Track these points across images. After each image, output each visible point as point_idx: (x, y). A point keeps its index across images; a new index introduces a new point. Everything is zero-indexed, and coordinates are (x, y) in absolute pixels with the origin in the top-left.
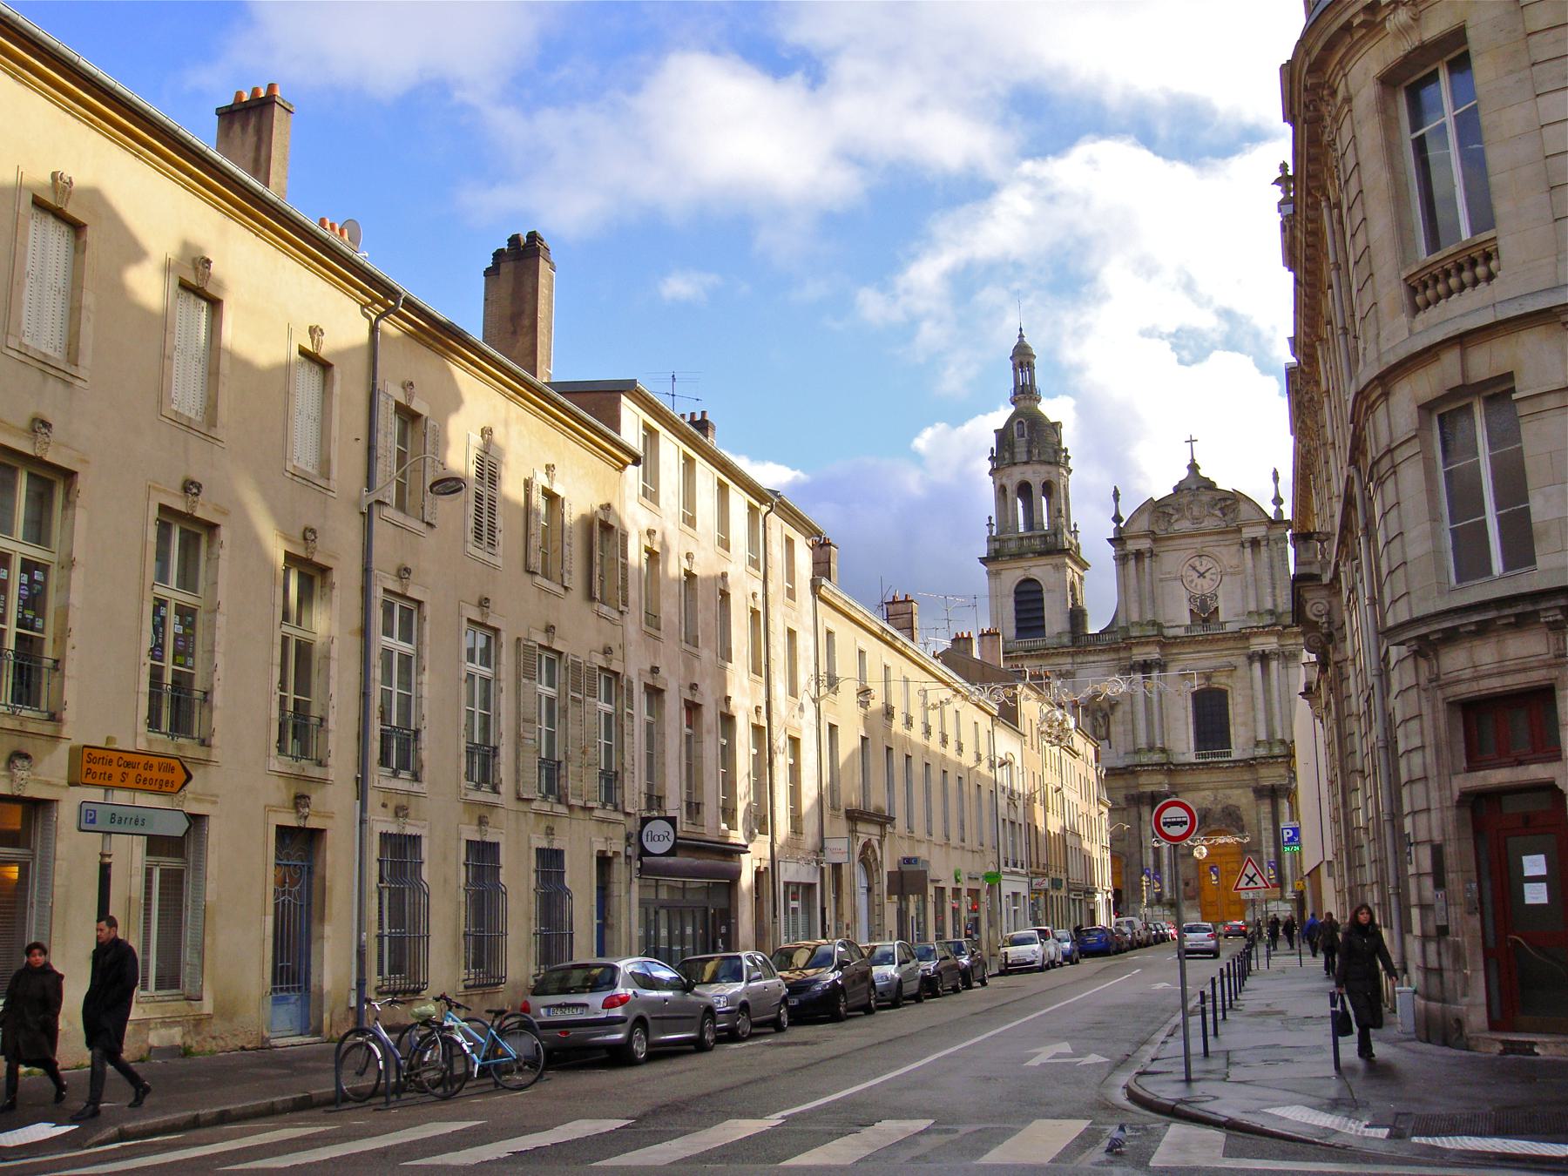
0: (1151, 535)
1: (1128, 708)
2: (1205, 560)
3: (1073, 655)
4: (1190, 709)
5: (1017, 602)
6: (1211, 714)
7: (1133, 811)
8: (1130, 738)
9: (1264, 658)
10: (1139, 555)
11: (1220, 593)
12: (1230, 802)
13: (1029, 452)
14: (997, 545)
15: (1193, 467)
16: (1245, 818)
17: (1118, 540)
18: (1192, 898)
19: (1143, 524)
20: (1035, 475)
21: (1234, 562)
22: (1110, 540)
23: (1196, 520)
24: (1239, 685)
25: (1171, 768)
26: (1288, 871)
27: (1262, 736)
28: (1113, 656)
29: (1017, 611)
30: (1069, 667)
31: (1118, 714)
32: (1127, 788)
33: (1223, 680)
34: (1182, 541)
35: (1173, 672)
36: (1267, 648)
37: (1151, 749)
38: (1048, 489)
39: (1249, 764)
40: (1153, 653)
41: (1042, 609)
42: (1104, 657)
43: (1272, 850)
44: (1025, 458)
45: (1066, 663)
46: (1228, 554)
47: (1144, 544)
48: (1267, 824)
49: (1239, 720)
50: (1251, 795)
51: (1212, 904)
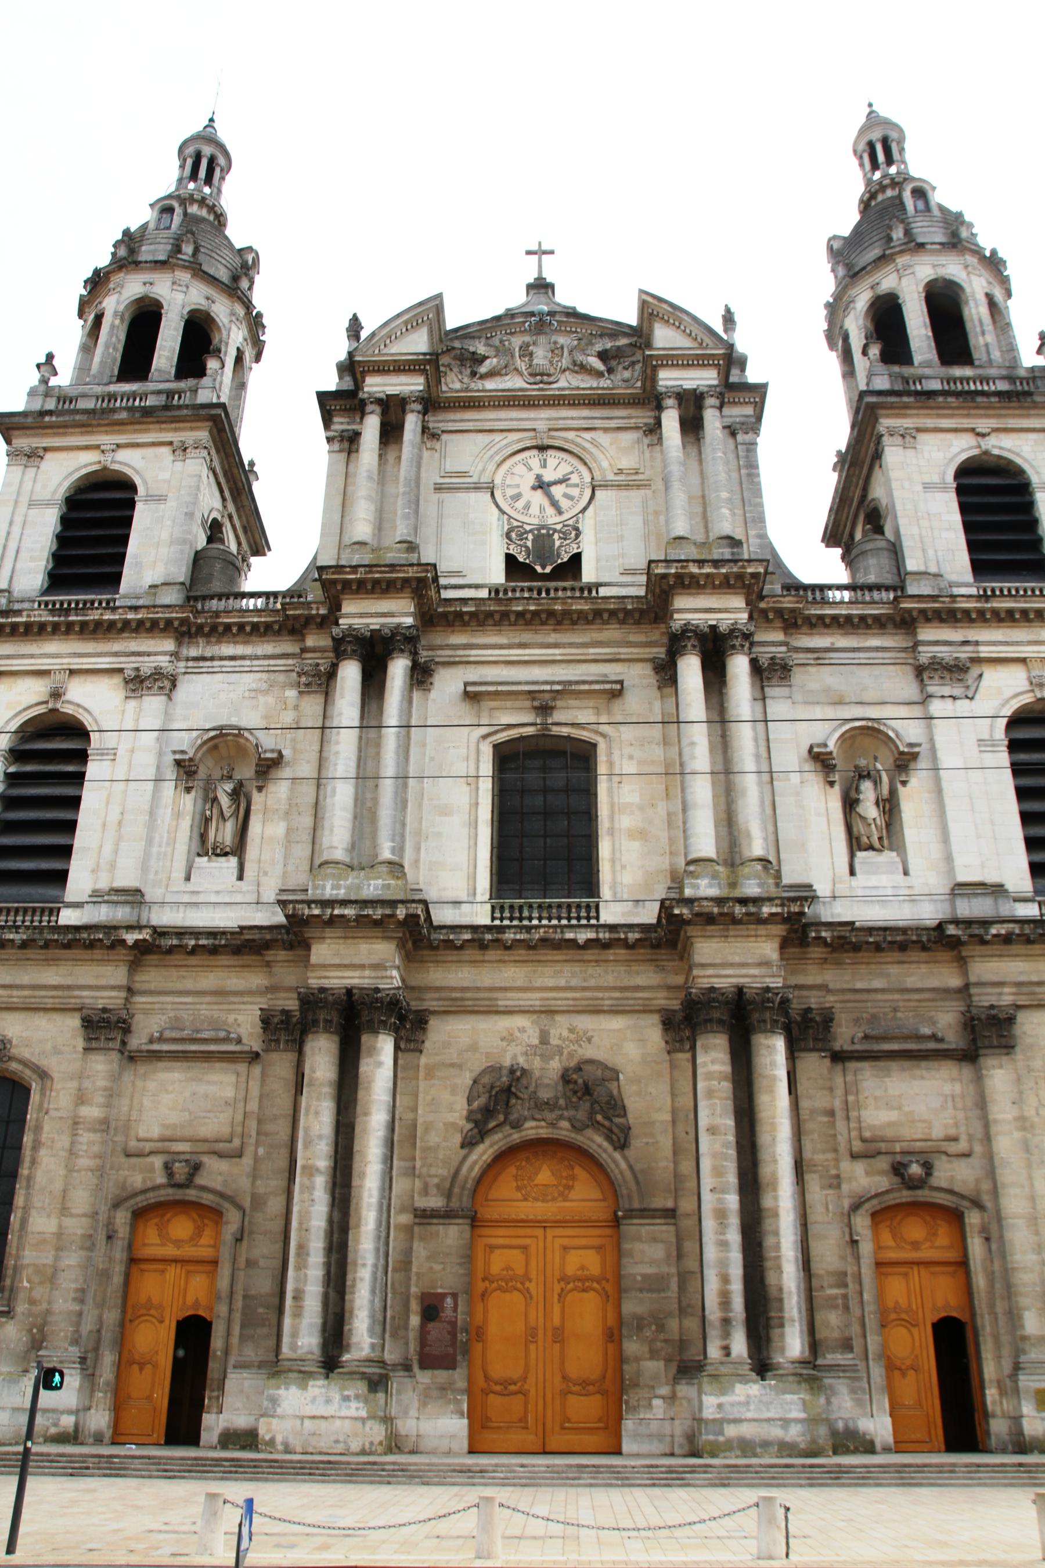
0: (428, 365)
1: (306, 769)
2: (553, 458)
3: (184, 631)
4: (486, 786)
5: (64, 520)
6: (544, 811)
7: (281, 1064)
8: (302, 851)
9: (715, 648)
10: (393, 412)
11: (588, 525)
12: (589, 1052)
13: (177, 249)
14: (51, 405)
15: (541, 287)
16: (634, 1104)
17: (339, 406)
18: (447, 1363)
19: (418, 343)
20: (178, 297)
21: (627, 462)
22: (323, 398)
23: (539, 375)
24: (627, 733)
25: (416, 932)
26: (788, 1277)
27: (705, 842)
28: (288, 646)
29: (61, 539)
30: (163, 661)
31: (279, 791)
32: (271, 989)
33: (585, 716)
34: (503, 414)
35: (448, 684)
36: (725, 621)
37: (362, 862)
38: (199, 339)
39: (670, 933)
40: (398, 612)
41: (124, 540)
42: (268, 648)
43: (733, 1200)
44: (162, 257)
45: (157, 652)
46: (614, 449)
47: (411, 385)
48: (716, 1115)
49: (625, 822)
50: (653, 1034)
51: (507, 1387)
